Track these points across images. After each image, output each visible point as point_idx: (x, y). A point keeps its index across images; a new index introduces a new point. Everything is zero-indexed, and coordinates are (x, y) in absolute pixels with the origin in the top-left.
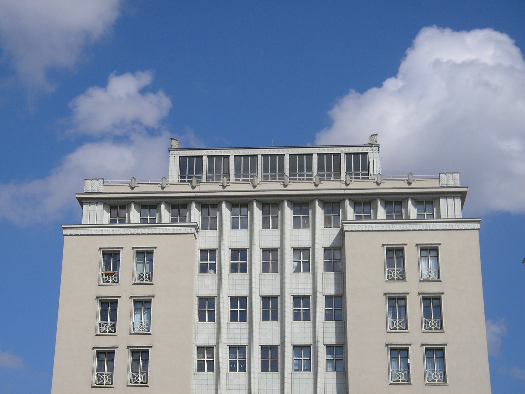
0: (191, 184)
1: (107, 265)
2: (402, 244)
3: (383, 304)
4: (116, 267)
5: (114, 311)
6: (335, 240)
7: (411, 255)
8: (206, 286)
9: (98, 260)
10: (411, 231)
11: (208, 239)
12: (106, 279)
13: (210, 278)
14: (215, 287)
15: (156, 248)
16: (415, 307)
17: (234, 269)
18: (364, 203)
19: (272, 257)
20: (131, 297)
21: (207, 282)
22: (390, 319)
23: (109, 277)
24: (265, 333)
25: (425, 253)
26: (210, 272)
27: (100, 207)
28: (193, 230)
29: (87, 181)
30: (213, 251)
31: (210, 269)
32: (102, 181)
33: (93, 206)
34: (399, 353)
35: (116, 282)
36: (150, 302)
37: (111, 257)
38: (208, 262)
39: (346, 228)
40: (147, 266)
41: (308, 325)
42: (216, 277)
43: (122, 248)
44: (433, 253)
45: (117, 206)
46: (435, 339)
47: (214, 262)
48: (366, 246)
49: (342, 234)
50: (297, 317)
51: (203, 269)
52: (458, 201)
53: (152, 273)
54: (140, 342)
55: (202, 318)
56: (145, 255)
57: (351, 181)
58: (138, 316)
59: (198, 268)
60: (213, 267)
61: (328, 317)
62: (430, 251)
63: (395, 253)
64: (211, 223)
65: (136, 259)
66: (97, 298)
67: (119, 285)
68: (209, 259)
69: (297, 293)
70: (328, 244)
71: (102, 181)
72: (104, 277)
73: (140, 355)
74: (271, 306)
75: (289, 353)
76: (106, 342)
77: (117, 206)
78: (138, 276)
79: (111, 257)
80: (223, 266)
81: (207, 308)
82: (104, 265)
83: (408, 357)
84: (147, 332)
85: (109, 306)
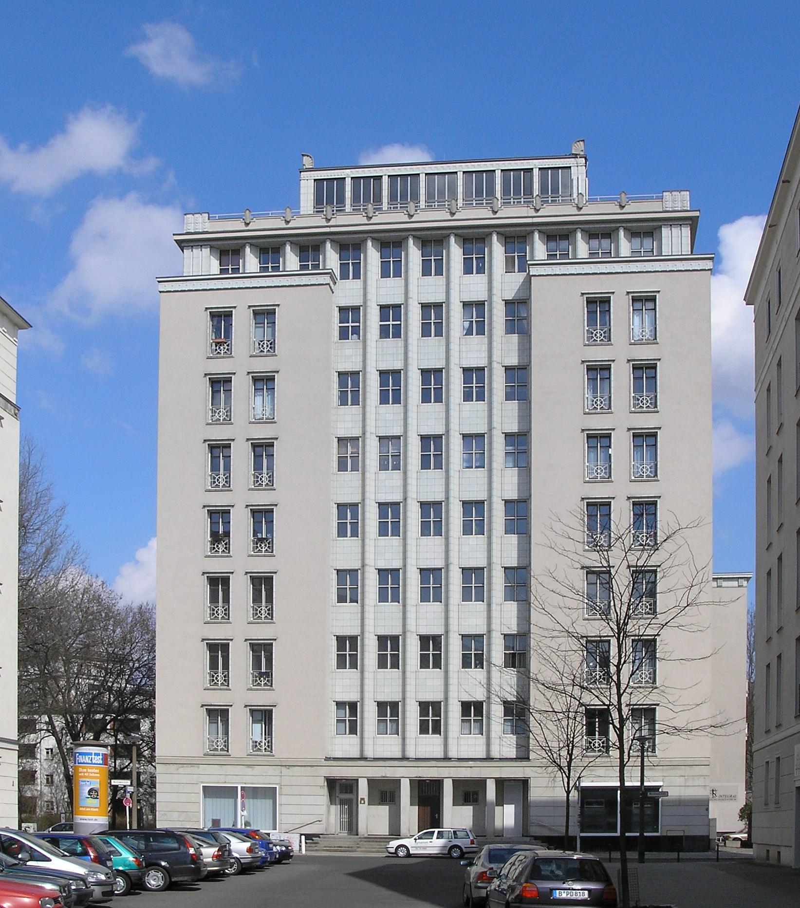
1: (217, 330)
8: (347, 356)
9: (205, 323)
11: (348, 292)
13: (352, 346)
14: (360, 359)
16: (622, 378)
17: (384, 332)
18: (559, 235)
21: (349, 352)
22: (588, 395)
25: (638, 305)
26: (353, 340)
27: (206, 251)
30: (356, 309)
32: (207, 215)
35: (229, 354)
36: (273, 379)
38: (350, 324)
42: (361, 345)
43: (235, 307)
44: (650, 305)
50: (467, 397)
56: (264, 315)
59: (336, 333)
60: (356, 331)
61: (509, 397)
64: (352, 268)
67: (232, 357)
68: (350, 318)
70: (509, 297)
71: (207, 215)
72: (214, 347)
74: (432, 581)
75: (456, 446)
76: (219, 433)
81: (350, 385)
83: (610, 447)
84: (271, 421)
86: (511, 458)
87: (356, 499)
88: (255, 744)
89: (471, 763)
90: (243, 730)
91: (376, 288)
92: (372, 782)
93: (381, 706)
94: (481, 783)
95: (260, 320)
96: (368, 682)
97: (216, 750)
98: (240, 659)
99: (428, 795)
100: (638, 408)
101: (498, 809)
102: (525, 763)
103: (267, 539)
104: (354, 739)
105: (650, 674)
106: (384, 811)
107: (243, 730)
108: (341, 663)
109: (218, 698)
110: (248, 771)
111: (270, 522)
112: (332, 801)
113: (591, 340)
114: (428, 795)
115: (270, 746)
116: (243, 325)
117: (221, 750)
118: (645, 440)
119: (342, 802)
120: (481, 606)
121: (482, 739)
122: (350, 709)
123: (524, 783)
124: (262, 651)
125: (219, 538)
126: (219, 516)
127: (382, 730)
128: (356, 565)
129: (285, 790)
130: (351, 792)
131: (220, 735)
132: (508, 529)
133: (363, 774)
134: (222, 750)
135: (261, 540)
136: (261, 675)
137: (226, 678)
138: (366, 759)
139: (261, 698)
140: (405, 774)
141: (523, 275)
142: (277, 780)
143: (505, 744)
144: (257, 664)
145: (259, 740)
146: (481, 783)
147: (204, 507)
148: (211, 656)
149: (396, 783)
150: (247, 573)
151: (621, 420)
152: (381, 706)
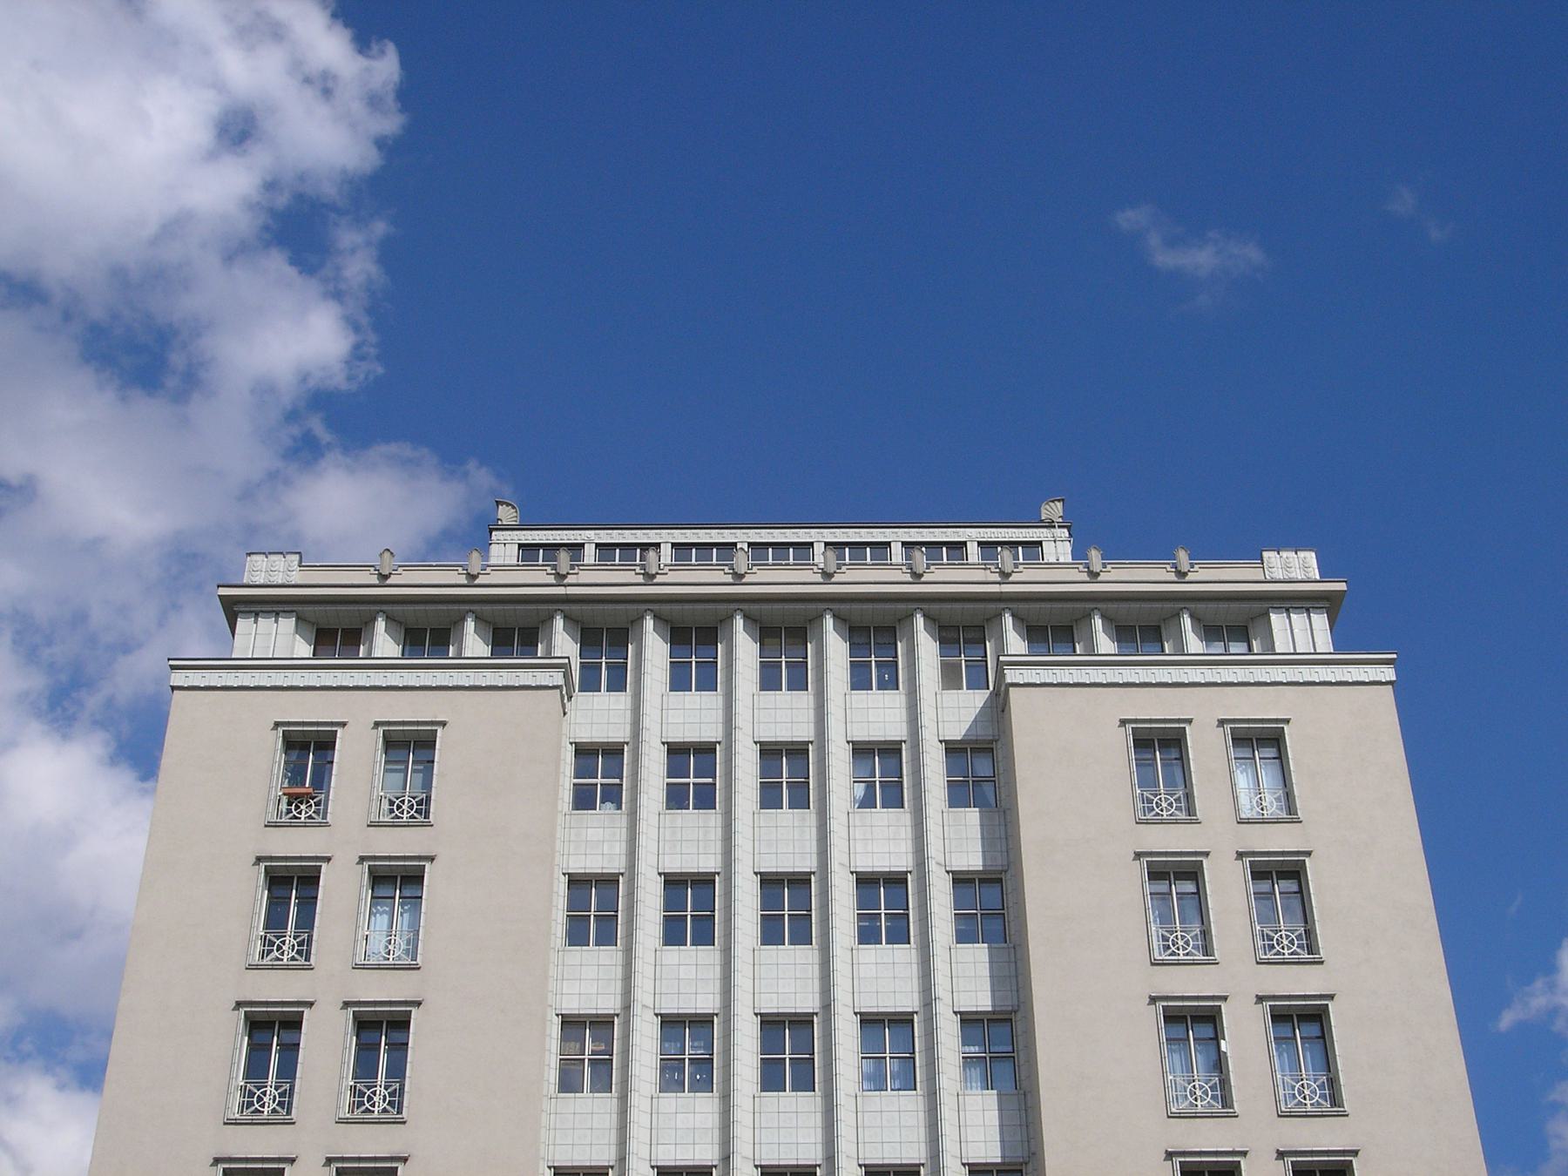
0: (554, 567)
1: (295, 773)
2: (1179, 721)
3: (1133, 883)
6: (975, 721)
7: (1207, 749)
9: (270, 756)
10: (1200, 690)
11: (600, 715)
12: (289, 811)
14: (620, 848)
15: (444, 724)
17: (676, 798)
19: (789, 770)
20: (362, 859)
23: (297, 807)
24: (777, 979)
27: (288, 624)
28: (557, 678)
29: (254, 557)
30: (613, 751)
31: (602, 802)
33: (265, 623)
34: (1193, 1021)
35: (320, 818)
37: (309, 748)
38: (599, 781)
40: (413, 779)
41: (904, 955)
43: (344, 724)
46: (1298, 983)
47: (617, 781)
48: (1071, 722)
49: (998, 707)
50: (867, 935)
51: (584, 799)
52: (1320, 621)
53: (428, 798)
54: (381, 990)
55: (577, 936)
57: (1016, 566)
58: (382, 921)
59: (567, 796)
62: (1260, 740)
63: (1160, 745)
65: (381, 757)
66: (259, 859)
67: (327, 825)
68: (600, 772)
69: (867, 864)
70: (957, 732)
72: (284, 807)
73: (381, 1031)
75: (847, 1034)
76: (277, 988)
77: (335, 628)
78: (386, 806)
79: (309, 748)
80: (644, 786)
81: (594, 906)
82: (285, 776)
85: (291, 886)
86: (976, 1073)
95: (397, 754)
100: (1269, 954)
113: (1148, 815)
116: (357, 766)
118: (1301, 1021)
141: (979, 698)
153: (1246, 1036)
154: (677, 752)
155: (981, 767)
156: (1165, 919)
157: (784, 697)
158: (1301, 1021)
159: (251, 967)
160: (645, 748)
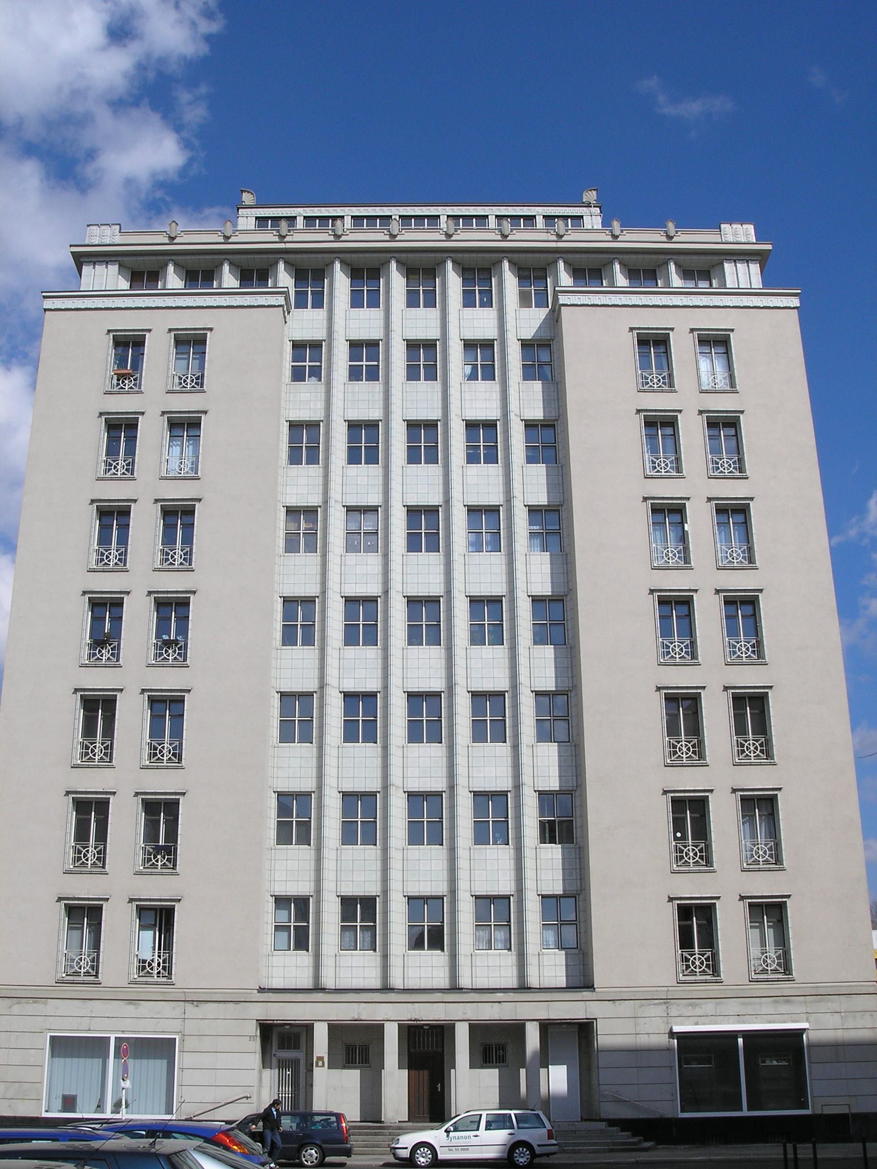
0: (278, 231)
1: (121, 361)
4: (137, 364)
5: (132, 440)
7: (682, 346)
11: (307, 323)
12: (118, 384)
15: (211, 329)
17: (355, 374)
19: (424, 356)
20: (163, 413)
21: (305, 396)
23: (123, 382)
24: (418, 484)
27: (114, 269)
28: (281, 300)
29: (91, 227)
30: (316, 345)
31: (309, 377)
32: (118, 227)
33: (100, 269)
34: (669, 513)
37: (129, 346)
39: (563, 299)
40: (193, 363)
41: (494, 471)
43: (150, 331)
45: (143, 271)
47: (318, 364)
48: (599, 329)
49: (554, 319)
50: (472, 458)
51: (298, 375)
52: (755, 268)
53: (203, 375)
57: (567, 230)
58: (176, 450)
59: (287, 373)
62: (716, 342)
63: (652, 344)
65: (173, 351)
66: (101, 414)
68: (308, 357)
69: (472, 415)
70: (528, 335)
71: (118, 227)
72: (115, 382)
73: (178, 516)
75: (459, 518)
76: (115, 491)
78: (177, 380)
79: (129, 346)
80: (335, 367)
82: (115, 363)
85: (121, 429)
86: (537, 542)
87: (312, 590)
88: (143, 965)
89: (500, 996)
90: (125, 941)
91: (345, 318)
92: (335, 1029)
93: (348, 903)
94: (517, 1029)
95: (183, 349)
96: (329, 865)
97: (77, 974)
98: (126, 825)
99: (427, 1049)
101: (543, 1071)
102: (586, 994)
103: (176, 642)
104: (304, 959)
105: (770, 849)
106: (352, 1077)
107: (125, 941)
108: (284, 835)
109: (85, 888)
110: (130, 1010)
111: (183, 620)
112: (266, 1063)
113: (645, 387)
114: (427, 1049)
115: (167, 968)
116: (159, 353)
117: (85, 974)
119: (282, 1065)
120: (503, 750)
121: (509, 959)
122: (298, 911)
123: (584, 1030)
124: (161, 812)
125: (104, 639)
126: (106, 609)
127: (349, 943)
128: (311, 685)
129: (190, 1043)
130: (297, 1047)
131: (85, 949)
132: (537, 639)
133: (320, 1014)
134: (87, 974)
135: (168, 644)
136: (158, 850)
137: (101, 856)
138: (323, 990)
139: (157, 888)
140: (391, 1015)
142: (176, 1025)
143: (550, 966)
144: (151, 833)
145: (149, 958)
146: (517, 1029)
147: (84, 593)
148: (78, 821)
149: (376, 1030)
150: (143, 691)
151: (697, 484)
152: (348, 903)
153: (700, 521)
154: (355, 346)
155: (543, 356)
156: (654, 450)
157: (421, 312)
158: (734, 513)
159: (99, 479)
160: (335, 343)
